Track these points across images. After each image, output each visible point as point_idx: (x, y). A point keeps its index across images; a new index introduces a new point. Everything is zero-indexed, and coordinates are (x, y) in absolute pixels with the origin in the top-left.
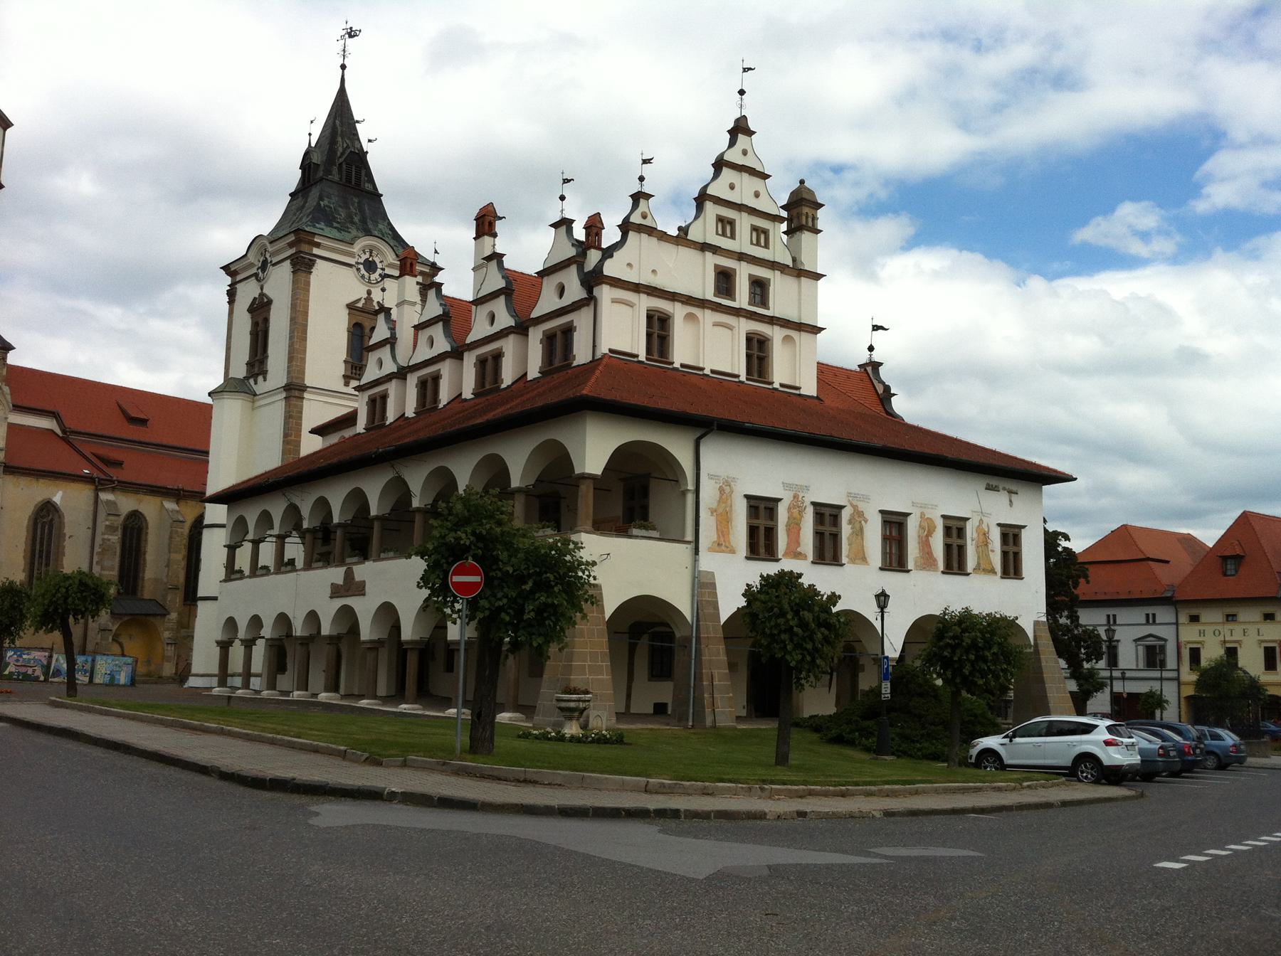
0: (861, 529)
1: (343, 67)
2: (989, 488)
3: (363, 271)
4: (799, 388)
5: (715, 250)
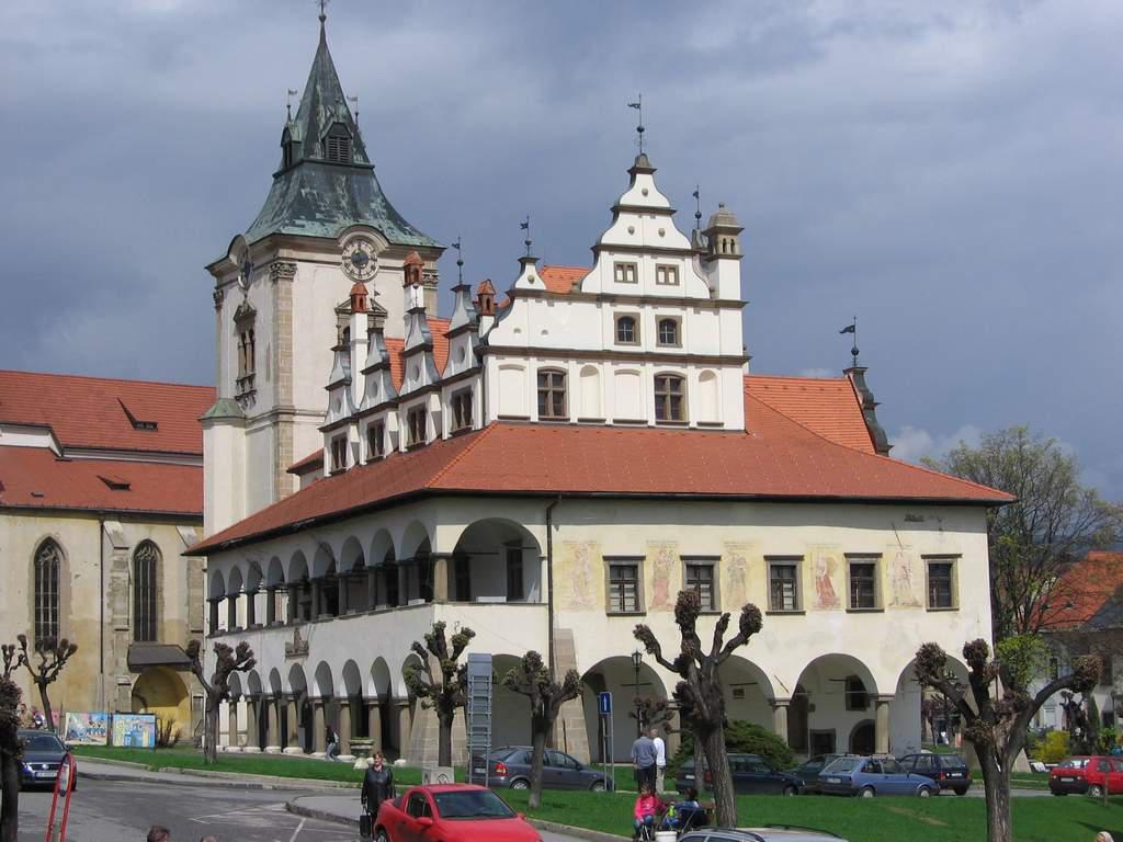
0: (743, 576)
1: (323, 19)
3: (352, 267)
4: (722, 424)
5: (612, 299)
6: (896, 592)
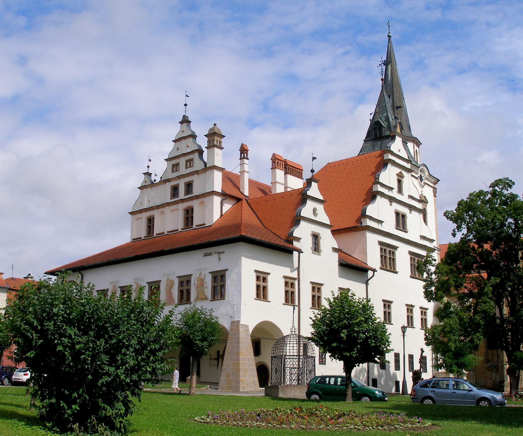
2: (206, 255)
4: (205, 224)
5: (169, 180)
6: (198, 293)
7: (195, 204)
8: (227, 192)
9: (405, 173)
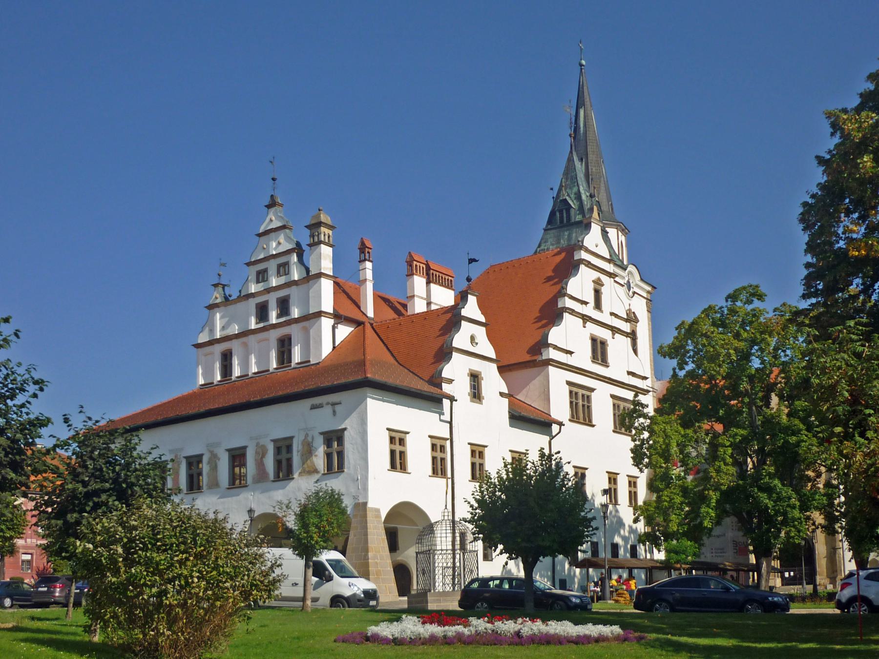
0: (216, 466)
2: (313, 407)
7: (294, 331)
8: (342, 312)
9: (604, 279)
